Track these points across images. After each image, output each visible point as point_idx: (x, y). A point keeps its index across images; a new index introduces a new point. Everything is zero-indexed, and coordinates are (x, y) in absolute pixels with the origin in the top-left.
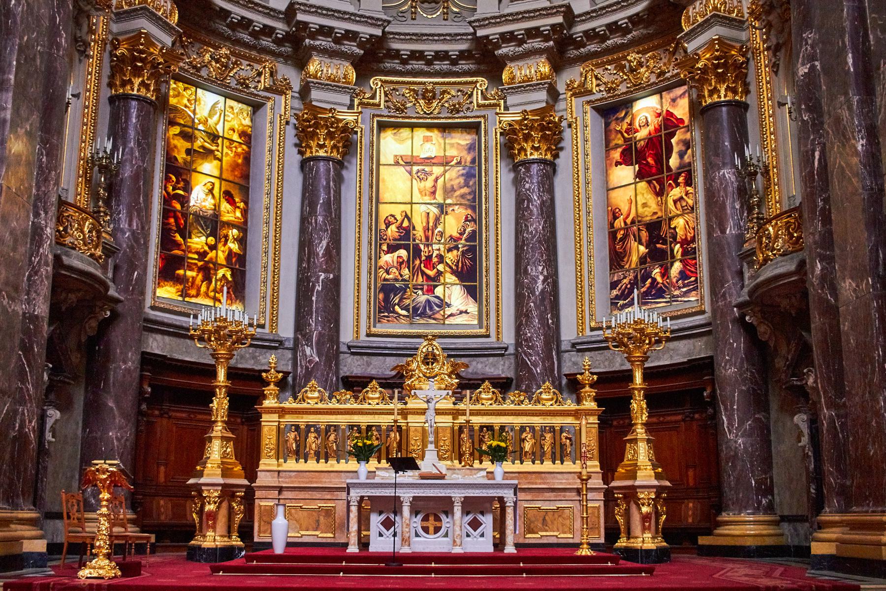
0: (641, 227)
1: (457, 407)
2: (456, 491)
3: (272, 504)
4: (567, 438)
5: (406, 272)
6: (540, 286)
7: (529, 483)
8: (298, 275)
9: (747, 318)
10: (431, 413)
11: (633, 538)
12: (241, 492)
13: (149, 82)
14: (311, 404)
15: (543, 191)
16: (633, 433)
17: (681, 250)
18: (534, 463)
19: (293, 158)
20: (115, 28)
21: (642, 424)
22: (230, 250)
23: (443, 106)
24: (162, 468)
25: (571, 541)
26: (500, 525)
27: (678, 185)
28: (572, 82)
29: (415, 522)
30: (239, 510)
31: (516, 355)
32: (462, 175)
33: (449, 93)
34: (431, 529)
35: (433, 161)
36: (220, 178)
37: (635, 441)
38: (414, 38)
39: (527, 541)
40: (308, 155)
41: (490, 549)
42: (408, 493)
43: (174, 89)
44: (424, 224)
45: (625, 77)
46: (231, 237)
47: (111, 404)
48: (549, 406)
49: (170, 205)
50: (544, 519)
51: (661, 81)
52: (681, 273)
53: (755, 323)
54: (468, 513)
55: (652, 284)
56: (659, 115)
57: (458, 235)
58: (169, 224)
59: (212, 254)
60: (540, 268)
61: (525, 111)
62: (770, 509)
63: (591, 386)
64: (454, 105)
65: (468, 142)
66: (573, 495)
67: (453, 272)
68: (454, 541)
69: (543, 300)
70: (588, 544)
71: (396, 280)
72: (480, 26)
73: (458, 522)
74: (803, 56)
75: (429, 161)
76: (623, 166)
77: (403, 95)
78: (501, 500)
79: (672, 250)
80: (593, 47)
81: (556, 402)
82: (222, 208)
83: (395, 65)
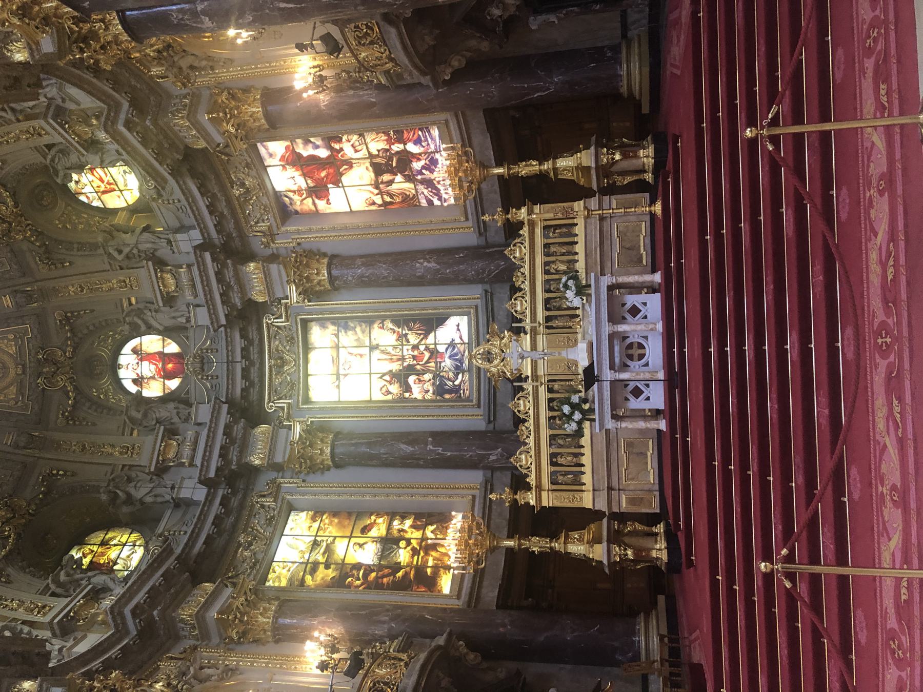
0: (380, 181)
1: (529, 331)
2: (603, 330)
3: (624, 497)
4: (554, 232)
5: (427, 376)
6: (432, 265)
9: (447, 78)
10: (536, 355)
11: (644, 167)
12: (614, 524)
13: (262, 608)
15: (355, 265)
16: (548, 172)
17: (396, 145)
20: (215, 640)
21: (540, 164)
22: (412, 526)
23: (288, 351)
25: (648, 224)
26: (635, 289)
27: (341, 149)
30: (631, 525)
32: (346, 332)
33: (278, 346)
34: (641, 351)
36: (350, 537)
37: (555, 169)
38: (230, 377)
39: (650, 264)
41: (658, 296)
42: (607, 374)
43: (274, 582)
44: (387, 362)
45: (255, 198)
46: (400, 527)
47: (542, 638)
50: (629, 249)
51: (254, 166)
52: (415, 144)
53: (451, 70)
54: (624, 318)
57: (395, 334)
58: (388, 583)
59: (414, 543)
60: (418, 265)
61: (287, 281)
62: (616, 49)
63: (507, 213)
64: (288, 341)
66: (606, 224)
67: (426, 337)
68: (652, 330)
70: (650, 206)
71: (434, 384)
72: (218, 320)
73: (633, 327)
74: (194, 23)
75: (336, 361)
76: (330, 197)
77: (281, 383)
78: (611, 288)
79: (397, 153)
80: (230, 226)
81: (522, 244)
82: (376, 535)
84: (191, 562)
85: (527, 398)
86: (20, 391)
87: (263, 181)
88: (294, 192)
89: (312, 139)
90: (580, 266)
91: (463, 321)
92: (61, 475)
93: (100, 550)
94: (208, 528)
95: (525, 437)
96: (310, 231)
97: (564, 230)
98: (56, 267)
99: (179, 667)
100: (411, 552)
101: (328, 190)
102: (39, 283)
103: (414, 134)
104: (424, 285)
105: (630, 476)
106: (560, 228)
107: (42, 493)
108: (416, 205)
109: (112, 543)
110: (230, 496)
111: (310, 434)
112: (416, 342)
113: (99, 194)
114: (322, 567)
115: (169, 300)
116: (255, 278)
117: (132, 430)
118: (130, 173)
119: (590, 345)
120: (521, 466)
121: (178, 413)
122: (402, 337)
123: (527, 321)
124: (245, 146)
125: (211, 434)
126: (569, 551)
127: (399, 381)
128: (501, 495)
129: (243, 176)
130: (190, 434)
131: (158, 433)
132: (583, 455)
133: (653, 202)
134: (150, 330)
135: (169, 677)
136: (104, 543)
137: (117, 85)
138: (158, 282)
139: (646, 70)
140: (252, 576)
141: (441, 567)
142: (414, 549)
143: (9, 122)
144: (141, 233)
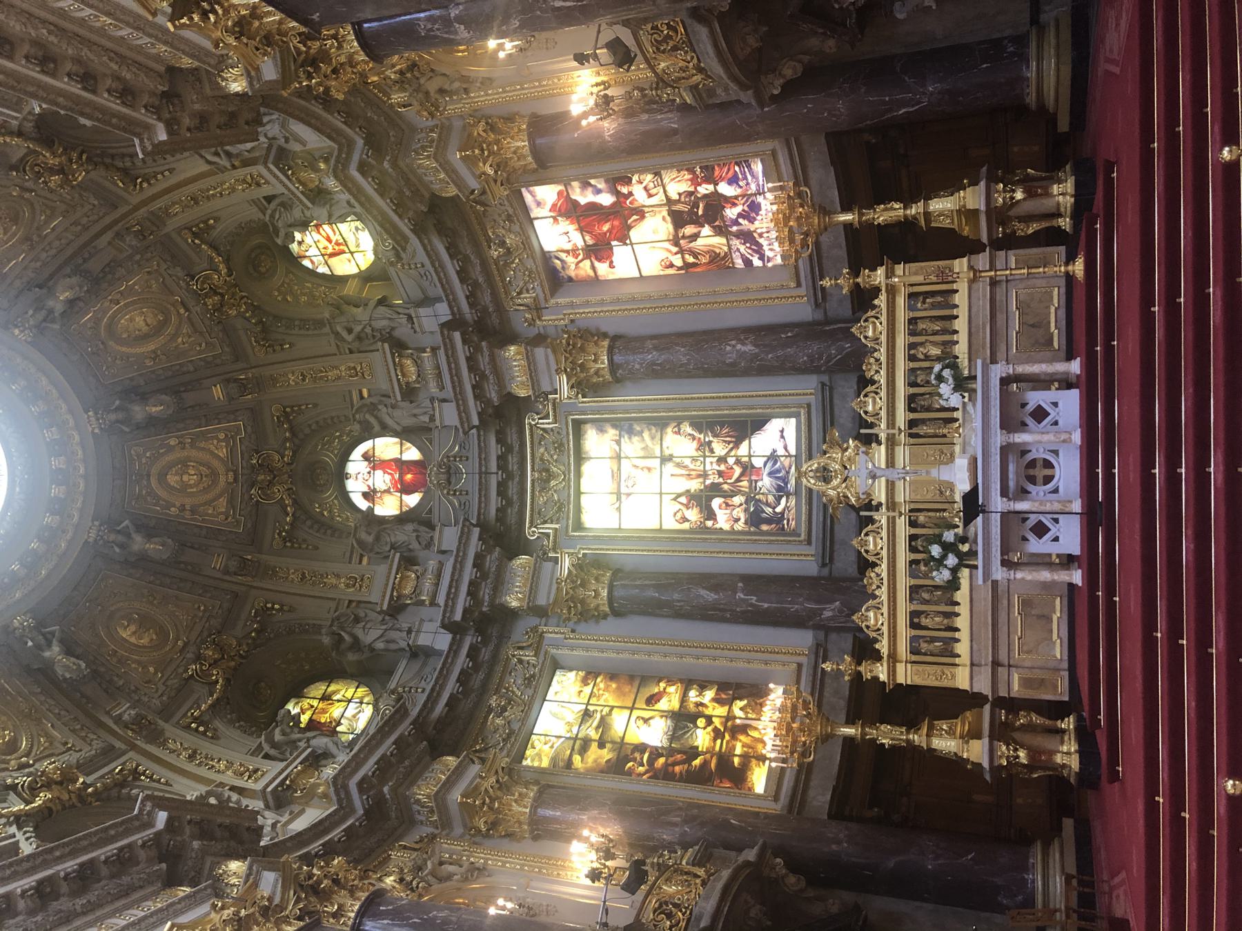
0: (681, 235)
1: (883, 440)
2: (992, 441)
3: (1016, 677)
4: (924, 302)
5: (738, 500)
6: (749, 348)
7: (984, 348)
8: (740, 623)
9: (776, 92)
10: (893, 474)
14: (883, 620)
15: (643, 348)
17: (704, 186)
18: (957, 342)
19: (611, 625)
20: (459, 830)
21: (905, 208)
22: (714, 700)
24: (976, 797)
25: (1063, 290)
26: (1041, 382)
27: (631, 194)
28: (526, 320)
29: (1037, 493)
31: (831, 371)
32: (630, 438)
34: (1048, 472)
35: (615, 470)
36: (632, 709)
37: (927, 214)
38: (483, 493)
40: (607, 609)
42: (996, 503)
43: (533, 760)
44: (683, 479)
46: (698, 699)
48: (882, 328)
49: (660, 770)
50: (1033, 326)
51: (518, 220)
54: (1024, 424)
55: (744, 217)
56: (555, 219)
57: (695, 442)
58: (681, 772)
59: (717, 722)
60: (728, 348)
61: (556, 371)
62: (1021, 41)
63: (857, 276)
64: (556, 448)
65: (594, 431)
67: (737, 445)
68: (1064, 441)
69: (765, 346)
70: (1067, 264)
73: (1037, 437)
74: (446, 33)
75: (617, 475)
76: (614, 259)
77: (545, 503)
78: (1005, 381)
79: (705, 196)
80: (486, 299)
82: (666, 709)
83: (512, 513)
84: (431, 728)
85: (879, 533)
86: (231, 502)
87: (528, 238)
88: (567, 252)
89: (593, 182)
90: (961, 349)
91: (790, 425)
92: (276, 610)
93: (321, 705)
94: (451, 686)
95: (874, 587)
96: (587, 304)
97: (939, 299)
98: (274, 351)
99: (414, 859)
100: (712, 734)
101: (611, 249)
102: (253, 370)
103: (729, 170)
104: (737, 376)
105: (1025, 648)
106: (933, 296)
107: (255, 630)
108: (729, 267)
109: (335, 698)
110: (479, 645)
111: (582, 570)
112: (723, 453)
113: (326, 257)
114: (594, 745)
115: (409, 393)
116: (516, 366)
117: (362, 556)
118: (363, 230)
119: (973, 461)
120: (868, 627)
121: (417, 537)
122: (705, 446)
123: (882, 426)
124: (506, 193)
125: (458, 566)
126: (933, 747)
127: (699, 505)
128: (838, 665)
129: (504, 232)
130: (432, 564)
131: (393, 561)
132: (958, 615)
133: (1070, 259)
134: (385, 431)
135: (402, 870)
136: (325, 698)
137: (351, 118)
138: (396, 370)
139: (1066, 71)
140: (505, 752)
141: (753, 757)
142: (716, 730)
143: (223, 170)
144: (375, 307)
